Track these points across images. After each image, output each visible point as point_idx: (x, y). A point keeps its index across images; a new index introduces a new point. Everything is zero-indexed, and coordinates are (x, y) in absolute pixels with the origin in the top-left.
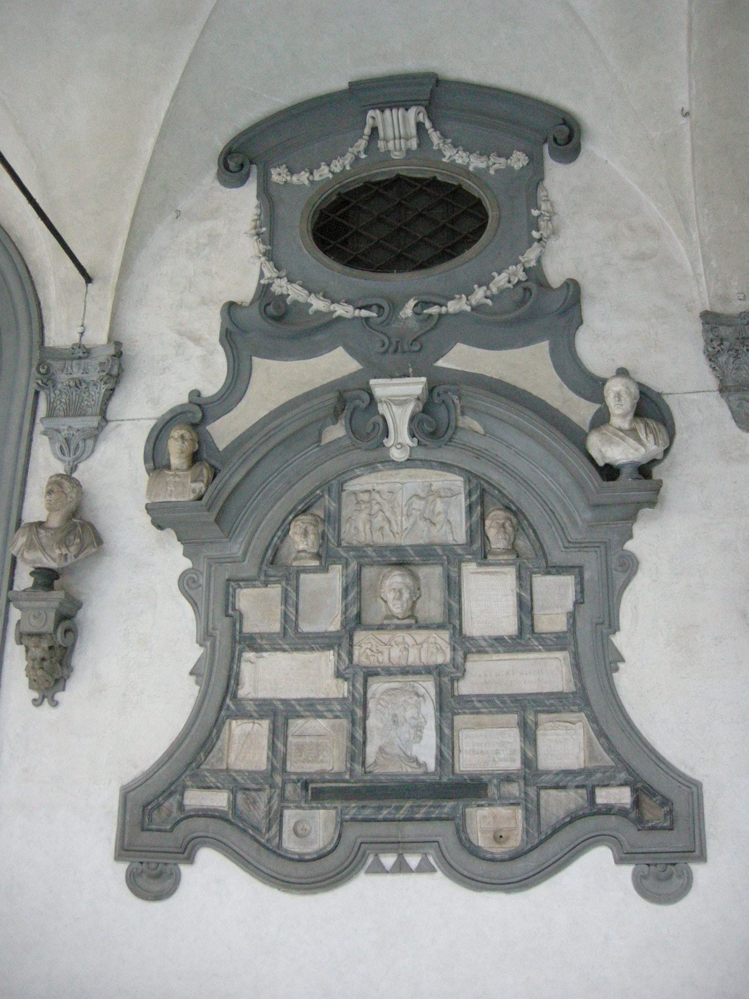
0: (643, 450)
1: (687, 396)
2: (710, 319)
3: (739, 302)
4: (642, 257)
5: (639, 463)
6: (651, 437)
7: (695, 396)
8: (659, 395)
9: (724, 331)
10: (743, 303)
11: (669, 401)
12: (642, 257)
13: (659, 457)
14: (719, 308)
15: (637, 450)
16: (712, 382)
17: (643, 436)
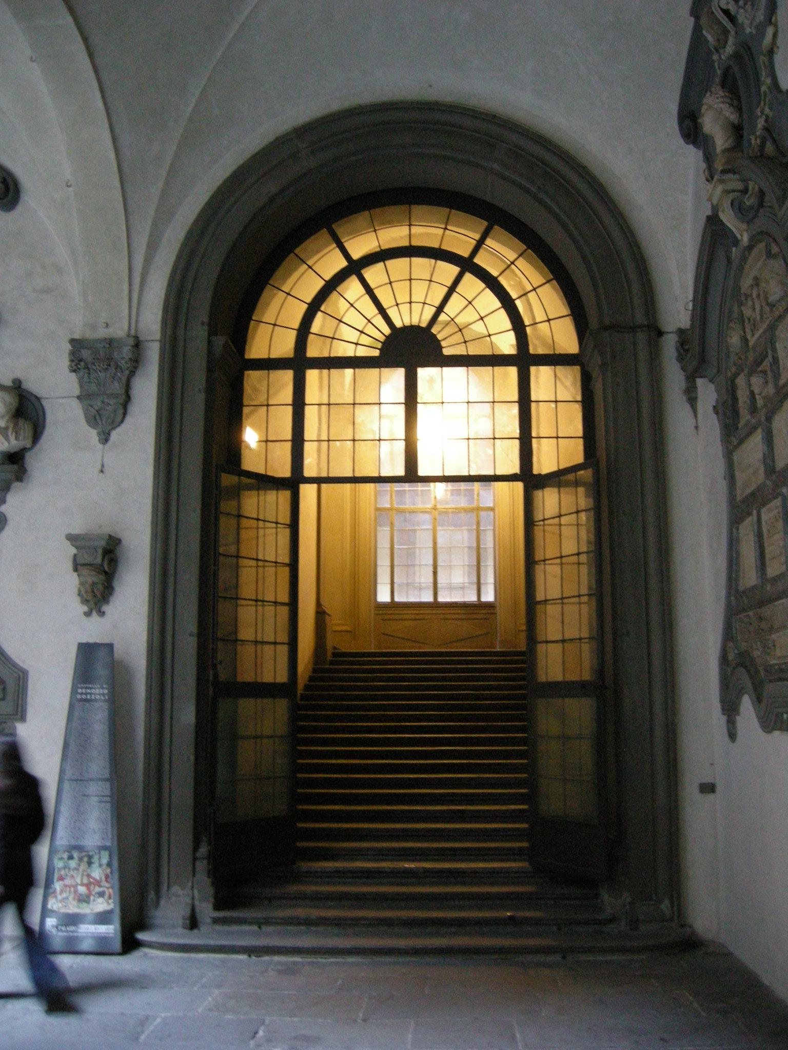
0: (6, 444)
1: (60, 401)
2: (77, 345)
3: (103, 329)
4: (47, 290)
5: (9, 452)
6: (14, 434)
7: (64, 401)
8: (38, 399)
9: (86, 354)
10: (106, 331)
11: (45, 403)
12: (47, 290)
13: (28, 445)
14: (90, 335)
15: (2, 444)
16: (76, 391)
17: (10, 434)
